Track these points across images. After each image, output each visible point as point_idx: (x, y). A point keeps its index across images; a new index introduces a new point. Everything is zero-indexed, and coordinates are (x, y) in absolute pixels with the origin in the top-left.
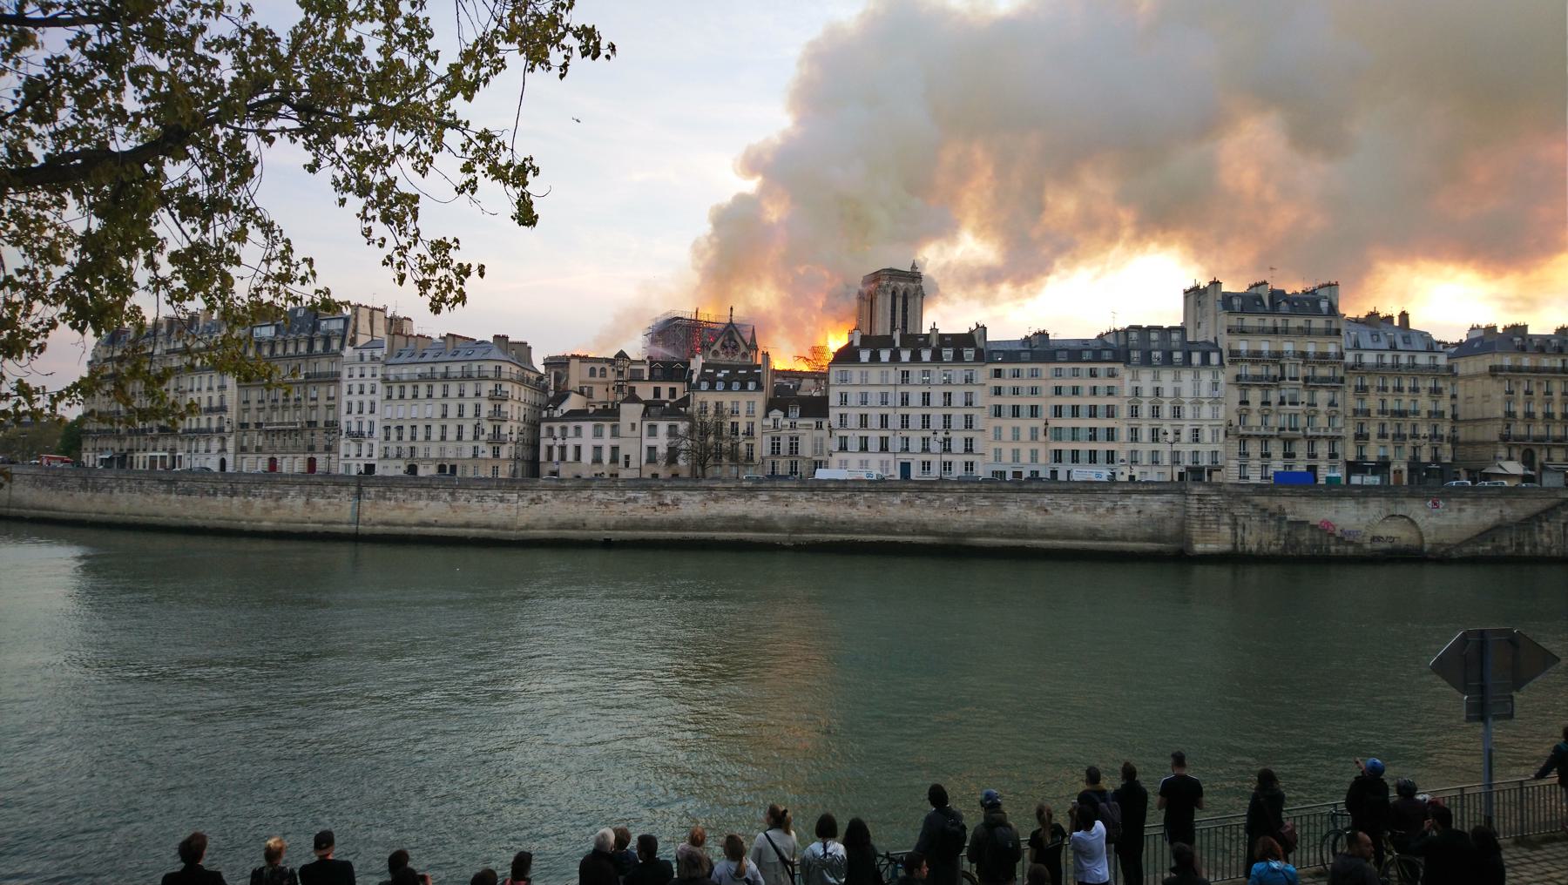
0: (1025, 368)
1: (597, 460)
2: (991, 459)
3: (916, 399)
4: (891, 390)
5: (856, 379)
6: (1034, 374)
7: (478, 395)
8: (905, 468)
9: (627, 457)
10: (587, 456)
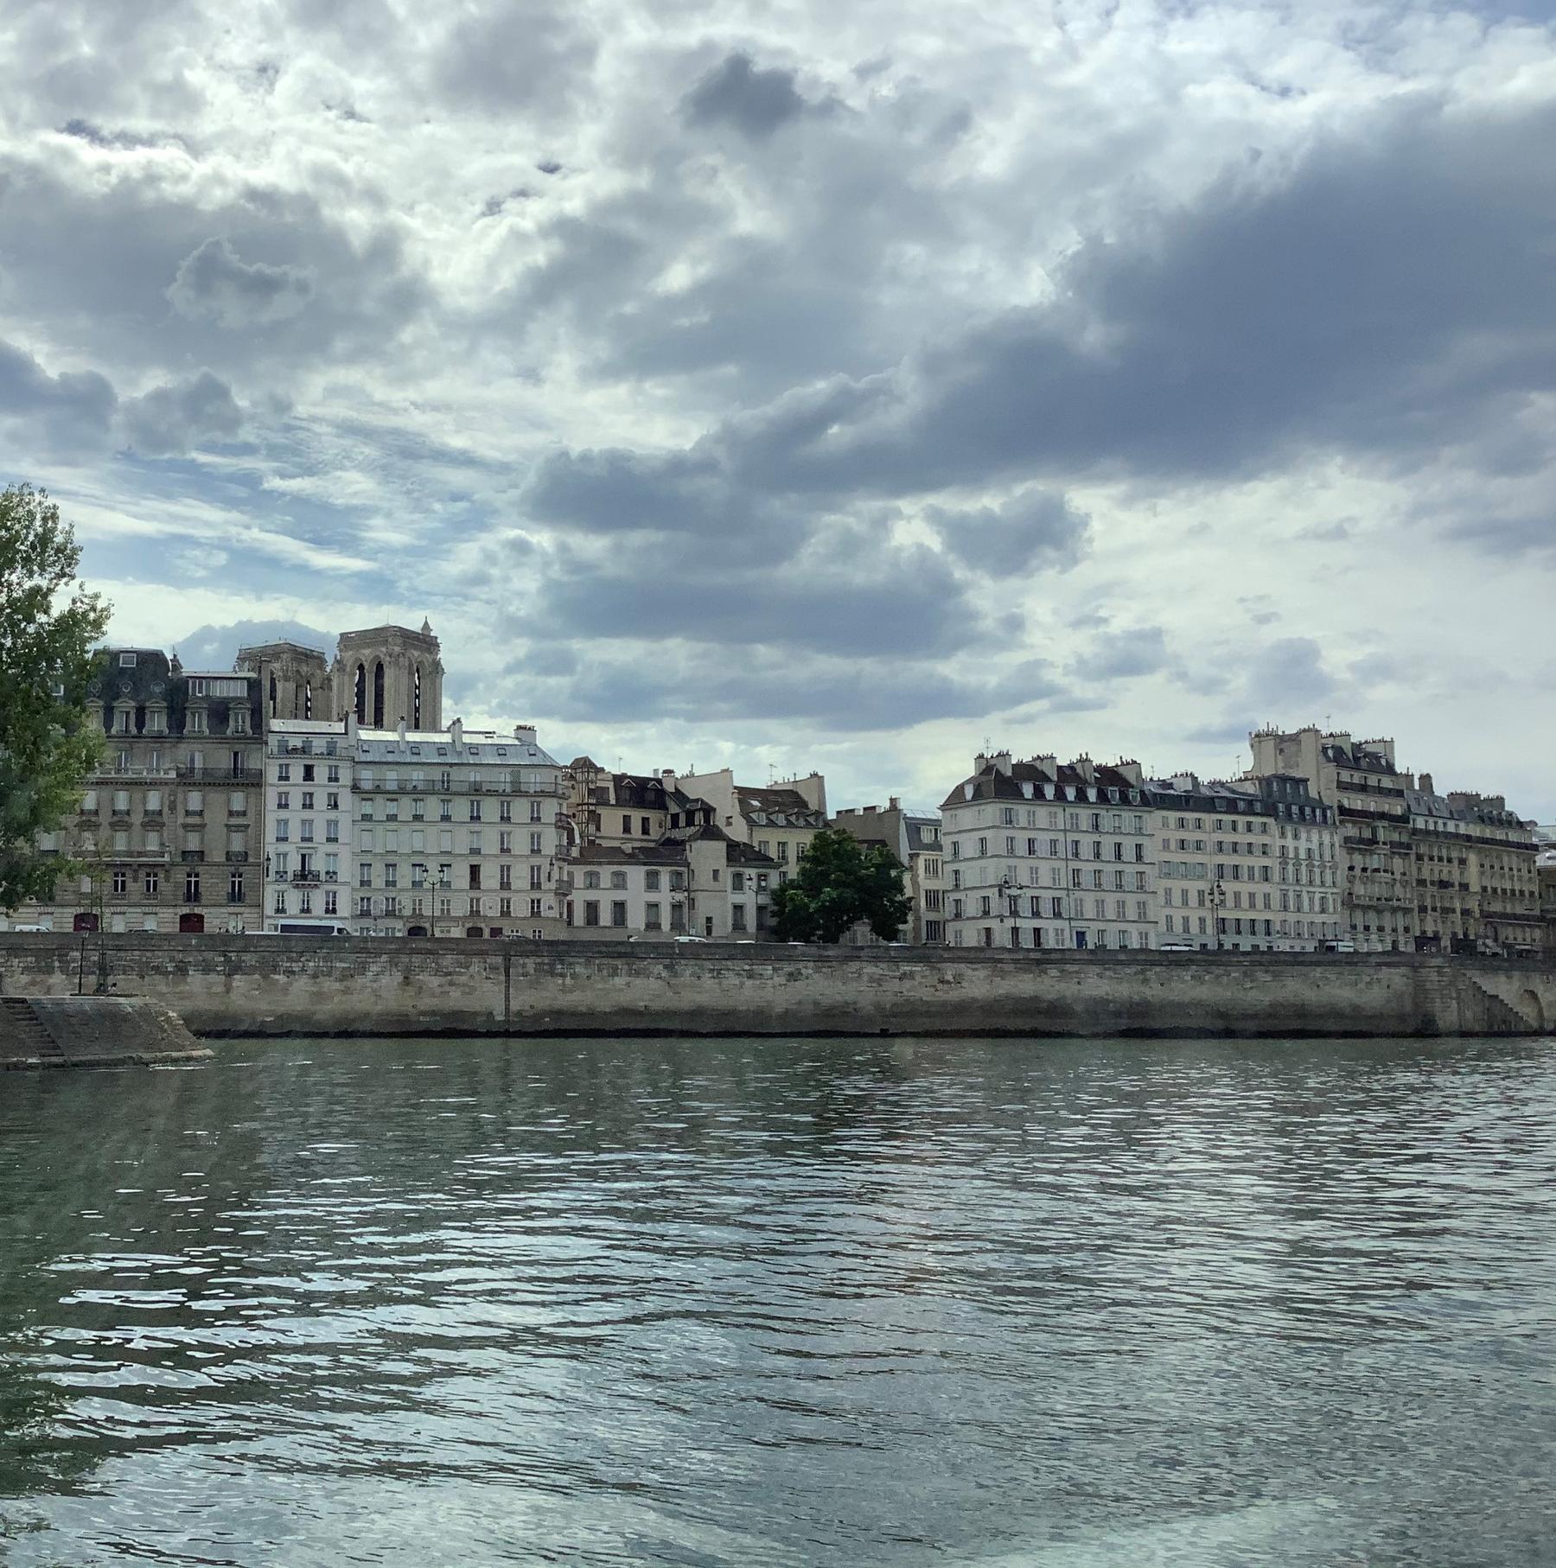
0: (1190, 816)
1: (653, 925)
2: (1162, 927)
3: (1086, 851)
4: (1061, 837)
5: (1023, 821)
6: (1199, 825)
7: (536, 819)
8: (1081, 936)
9: (709, 920)
10: (636, 919)
